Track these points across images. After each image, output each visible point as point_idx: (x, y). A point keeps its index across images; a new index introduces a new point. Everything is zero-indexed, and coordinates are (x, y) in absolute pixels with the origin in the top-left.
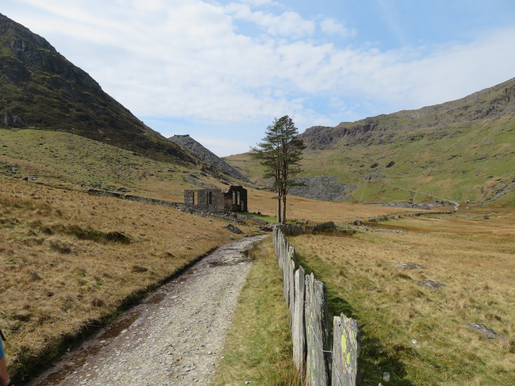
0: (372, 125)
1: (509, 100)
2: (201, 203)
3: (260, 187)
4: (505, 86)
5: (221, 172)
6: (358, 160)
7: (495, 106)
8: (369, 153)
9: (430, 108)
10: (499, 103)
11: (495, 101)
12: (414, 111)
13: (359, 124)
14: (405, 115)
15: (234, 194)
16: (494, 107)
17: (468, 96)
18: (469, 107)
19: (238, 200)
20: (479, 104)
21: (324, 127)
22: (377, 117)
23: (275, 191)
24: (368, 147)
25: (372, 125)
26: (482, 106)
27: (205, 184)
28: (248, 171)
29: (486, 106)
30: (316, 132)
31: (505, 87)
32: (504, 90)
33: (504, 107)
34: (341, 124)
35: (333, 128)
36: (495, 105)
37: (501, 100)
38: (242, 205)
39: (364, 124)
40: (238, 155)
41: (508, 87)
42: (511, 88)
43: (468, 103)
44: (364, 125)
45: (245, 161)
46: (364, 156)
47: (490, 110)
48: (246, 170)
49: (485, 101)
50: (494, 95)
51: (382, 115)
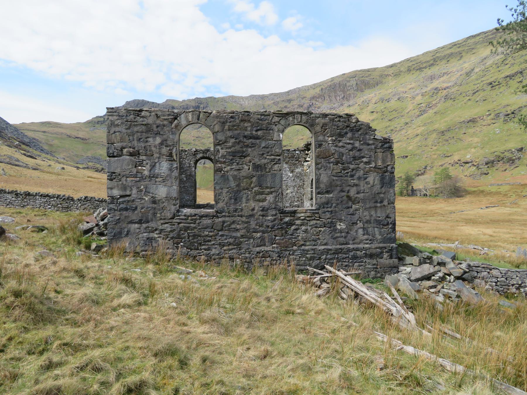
0: (202, 106)
1: (324, 99)
2: (237, 199)
3: (81, 166)
4: (320, 86)
5: (15, 141)
6: (189, 142)
7: (314, 103)
8: (200, 135)
9: (257, 97)
10: (317, 101)
11: (313, 98)
12: (242, 98)
13: (189, 103)
14: (234, 100)
16: (312, 103)
17: (291, 90)
18: (292, 100)
20: (301, 99)
21: (148, 102)
22: (206, 98)
23: (102, 172)
24: (198, 130)
25: (202, 106)
26: (303, 101)
28: (51, 145)
29: (307, 101)
30: (139, 106)
31: (321, 87)
32: (320, 89)
33: (321, 105)
34: (167, 100)
35: (159, 104)
36: (314, 102)
37: (318, 98)
39: (193, 104)
40: (32, 123)
41: (322, 87)
42: (326, 88)
43: (290, 97)
44: (194, 105)
45: (44, 132)
46: (195, 138)
47: (310, 106)
48: (47, 144)
49: (305, 97)
50: (312, 93)
51: (211, 97)
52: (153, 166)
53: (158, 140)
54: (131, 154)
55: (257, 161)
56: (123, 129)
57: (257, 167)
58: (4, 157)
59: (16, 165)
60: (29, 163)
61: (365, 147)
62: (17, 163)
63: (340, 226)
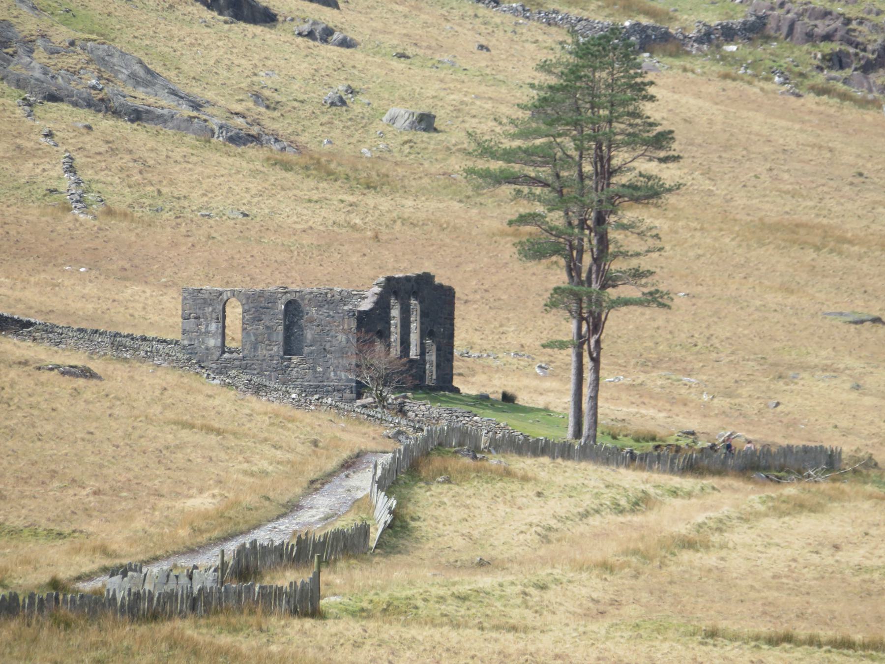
2: (255, 349)
15: (395, 312)
19: (414, 338)
27: (29, 45)
38: (432, 357)
52: (207, 326)
53: (211, 309)
54: (196, 318)
55: (268, 323)
56: (190, 302)
57: (268, 328)
58: (70, 61)
59: (137, 116)
60: (210, 95)
61: (336, 315)
62: (142, 98)
63: (319, 369)
